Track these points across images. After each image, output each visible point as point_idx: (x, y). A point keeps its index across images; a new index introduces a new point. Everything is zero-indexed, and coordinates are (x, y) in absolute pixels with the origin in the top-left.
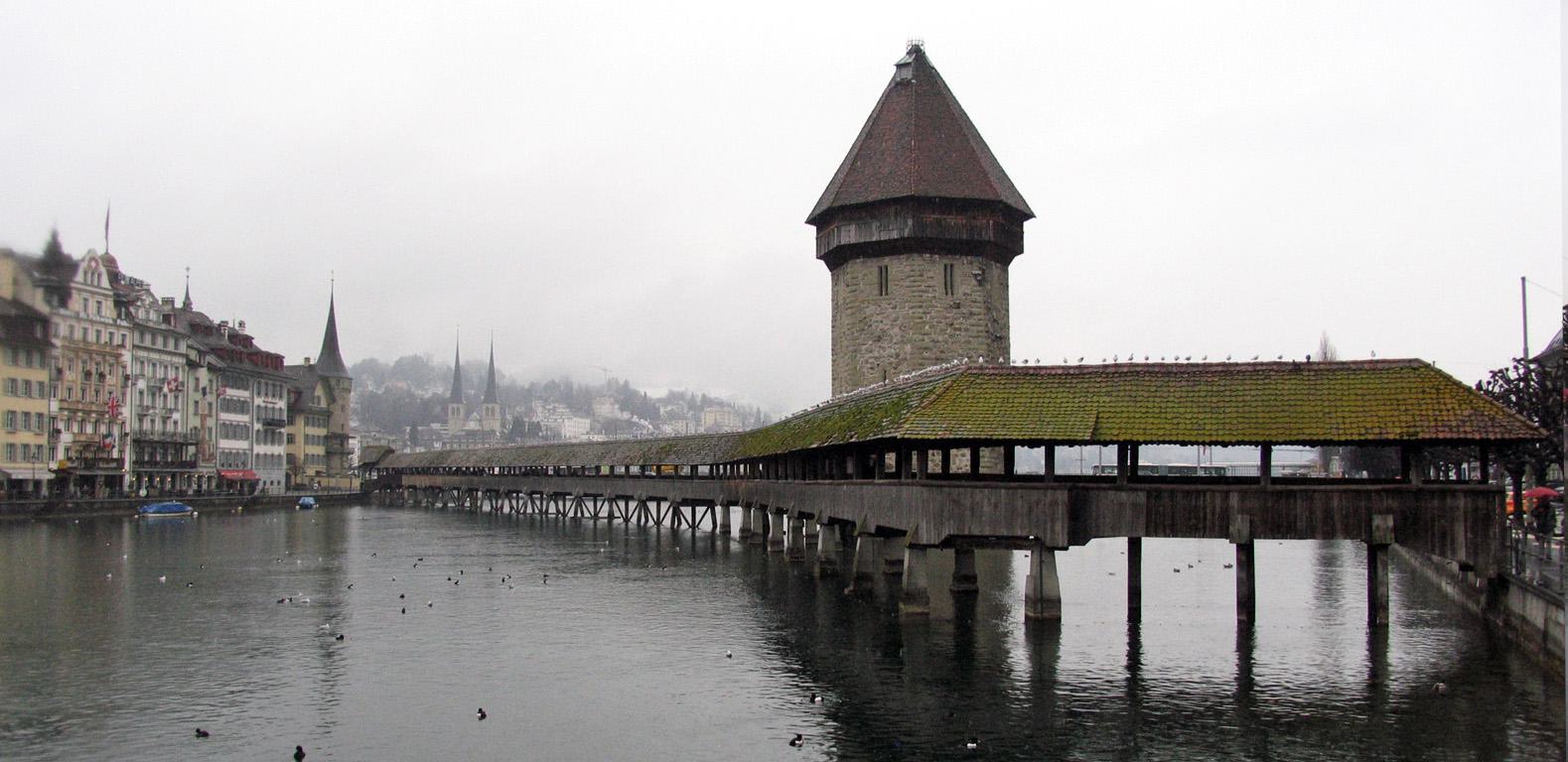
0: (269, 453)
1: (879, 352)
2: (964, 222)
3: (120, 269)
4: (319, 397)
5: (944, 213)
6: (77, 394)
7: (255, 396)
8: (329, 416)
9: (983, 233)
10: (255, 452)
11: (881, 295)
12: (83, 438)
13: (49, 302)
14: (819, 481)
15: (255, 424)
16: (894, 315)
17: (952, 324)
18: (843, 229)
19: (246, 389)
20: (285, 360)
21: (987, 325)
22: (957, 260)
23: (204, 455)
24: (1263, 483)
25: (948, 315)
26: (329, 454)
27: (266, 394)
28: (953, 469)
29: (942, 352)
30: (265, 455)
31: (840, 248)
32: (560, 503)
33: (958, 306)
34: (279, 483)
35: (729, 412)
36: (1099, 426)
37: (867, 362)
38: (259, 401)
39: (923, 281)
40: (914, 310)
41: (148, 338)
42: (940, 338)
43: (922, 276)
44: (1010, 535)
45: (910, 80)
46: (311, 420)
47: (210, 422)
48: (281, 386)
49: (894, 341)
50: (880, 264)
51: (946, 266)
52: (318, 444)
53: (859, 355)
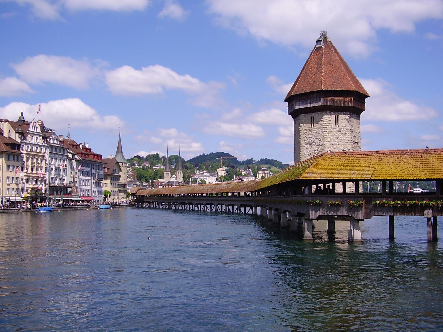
2: (342, 99)
3: (44, 126)
4: (116, 170)
6: (30, 171)
7: (92, 170)
9: (349, 103)
10: (92, 190)
11: (312, 127)
12: (31, 186)
13: (21, 138)
14: (281, 196)
17: (338, 138)
18: (297, 103)
19: (89, 167)
20: (102, 156)
21: (351, 138)
22: (340, 113)
23: (74, 191)
24: (437, 195)
25: (337, 134)
27: (96, 169)
29: (335, 148)
32: (183, 206)
34: (101, 201)
38: (93, 171)
39: (327, 122)
40: (323, 133)
41: (54, 149)
42: (334, 144)
43: (327, 120)
44: (342, 215)
46: (113, 178)
48: (101, 166)
50: (311, 116)
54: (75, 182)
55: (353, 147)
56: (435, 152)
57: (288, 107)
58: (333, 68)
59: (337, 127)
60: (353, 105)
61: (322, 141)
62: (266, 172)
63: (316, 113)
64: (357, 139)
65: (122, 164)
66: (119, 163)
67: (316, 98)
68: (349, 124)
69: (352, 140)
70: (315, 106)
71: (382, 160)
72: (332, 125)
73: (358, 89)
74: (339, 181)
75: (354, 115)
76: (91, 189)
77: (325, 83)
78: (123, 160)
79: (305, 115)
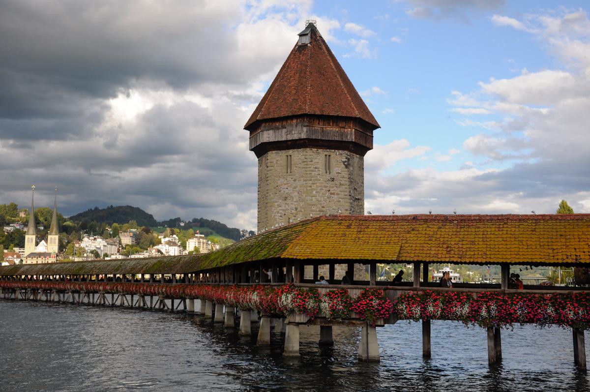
1: (285, 206)
5: (325, 125)
9: (348, 137)
11: (287, 173)
16: (294, 185)
21: (350, 192)
24: (502, 288)
25: (327, 185)
29: (323, 207)
31: (263, 144)
33: (333, 180)
36: (402, 252)
37: (278, 212)
39: (312, 165)
45: (307, 45)
49: (295, 200)
51: (326, 155)
53: (273, 208)
55: (352, 206)
56: (498, 219)
57: (250, 138)
58: (324, 80)
59: (328, 173)
60: (354, 141)
61: (304, 196)
63: (295, 150)
64: (359, 194)
67: (296, 126)
68: (346, 169)
69: (350, 195)
70: (294, 139)
71: (413, 230)
72: (319, 171)
73: (363, 116)
74: (341, 262)
75: (355, 157)
77: (312, 103)
79: (277, 153)
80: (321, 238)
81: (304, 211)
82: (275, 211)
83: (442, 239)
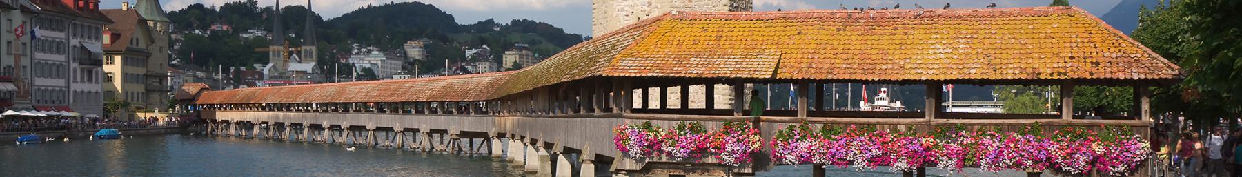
0: (86, 90)
7: (71, 37)
8: (147, 57)
10: (72, 90)
15: (71, 62)
19: (61, 31)
26: (148, 91)
28: (691, 106)
30: (83, 92)
35: (527, 55)
38: (74, 42)
47: (25, 61)
52: (138, 83)
54: (22, 69)
62: (524, 52)
65: (155, 24)
66: (145, 21)
71: (799, 33)
74: (697, 81)
76: (69, 87)
78: (159, 15)
80: (663, 46)
81: (662, 7)
82: (619, 7)
83: (841, 47)
